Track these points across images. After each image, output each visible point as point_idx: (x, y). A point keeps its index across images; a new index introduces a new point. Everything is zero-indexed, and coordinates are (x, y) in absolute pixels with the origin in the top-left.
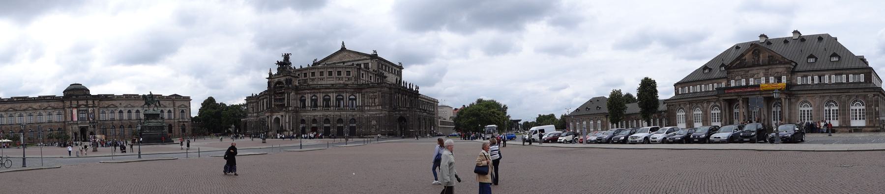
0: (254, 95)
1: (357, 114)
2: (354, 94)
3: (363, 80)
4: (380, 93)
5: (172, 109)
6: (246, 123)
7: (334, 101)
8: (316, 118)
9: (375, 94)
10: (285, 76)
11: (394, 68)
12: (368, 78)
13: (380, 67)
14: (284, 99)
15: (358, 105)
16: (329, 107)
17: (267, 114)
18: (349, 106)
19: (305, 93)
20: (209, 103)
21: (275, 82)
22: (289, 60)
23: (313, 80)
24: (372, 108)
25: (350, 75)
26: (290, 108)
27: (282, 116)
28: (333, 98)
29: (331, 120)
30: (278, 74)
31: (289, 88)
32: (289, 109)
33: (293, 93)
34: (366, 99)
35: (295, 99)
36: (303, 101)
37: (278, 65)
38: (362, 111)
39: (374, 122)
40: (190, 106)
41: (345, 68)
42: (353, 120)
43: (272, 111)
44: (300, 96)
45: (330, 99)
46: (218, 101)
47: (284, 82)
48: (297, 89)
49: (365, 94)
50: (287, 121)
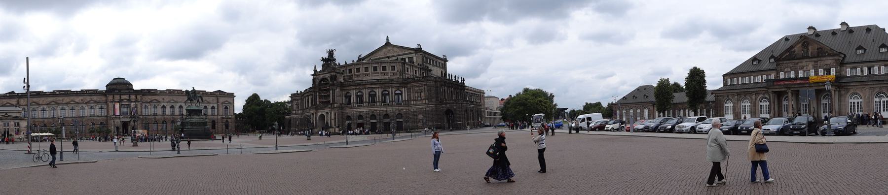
0: (299, 92)
1: (403, 109)
2: (400, 89)
3: (408, 75)
4: (426, 87)
5: (215, 106)
6: (290, 120)
7: (380, 97)
8: (361, 114)
9: (421, 88)
10: (329, 72)
11: (439, 61)
12: (413, 71)
13: (425, 61)
14: (329, 95)
15: (404, 99)
16: (374, 102)
17: (312, 111)
18: (395, 101)
19: (351, 89)
20: (254, 99)
21: (320, 78)
22: (334, 56)
23: (358, 76)
24: (418, 103)
25: (395, 70)
26: (336, 105)
27: (327, 113)
28: (379, 93)
29: (377, 116)
30: (323, 70)
31: (334, 85)
32: (334, 105)
33: (338, 90)
34: (412, 94)
35: (339, 96)
36: (348, 97)
37: (322, 62)
38: (408, 106)
39: (420, 116)
40: (234, 103)
41: (390, 62)
42: (400, 115)
43: (317, 109)
44: (346, 92)
45: (375, 95)
46: (262, 98)
47: (329, 79)
48: (342, 86)
49: (410, 89)
50: (333, 117)
